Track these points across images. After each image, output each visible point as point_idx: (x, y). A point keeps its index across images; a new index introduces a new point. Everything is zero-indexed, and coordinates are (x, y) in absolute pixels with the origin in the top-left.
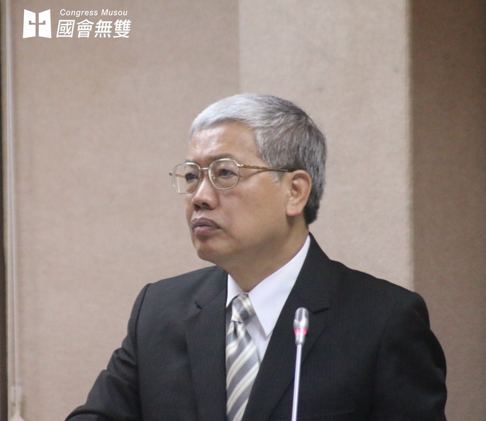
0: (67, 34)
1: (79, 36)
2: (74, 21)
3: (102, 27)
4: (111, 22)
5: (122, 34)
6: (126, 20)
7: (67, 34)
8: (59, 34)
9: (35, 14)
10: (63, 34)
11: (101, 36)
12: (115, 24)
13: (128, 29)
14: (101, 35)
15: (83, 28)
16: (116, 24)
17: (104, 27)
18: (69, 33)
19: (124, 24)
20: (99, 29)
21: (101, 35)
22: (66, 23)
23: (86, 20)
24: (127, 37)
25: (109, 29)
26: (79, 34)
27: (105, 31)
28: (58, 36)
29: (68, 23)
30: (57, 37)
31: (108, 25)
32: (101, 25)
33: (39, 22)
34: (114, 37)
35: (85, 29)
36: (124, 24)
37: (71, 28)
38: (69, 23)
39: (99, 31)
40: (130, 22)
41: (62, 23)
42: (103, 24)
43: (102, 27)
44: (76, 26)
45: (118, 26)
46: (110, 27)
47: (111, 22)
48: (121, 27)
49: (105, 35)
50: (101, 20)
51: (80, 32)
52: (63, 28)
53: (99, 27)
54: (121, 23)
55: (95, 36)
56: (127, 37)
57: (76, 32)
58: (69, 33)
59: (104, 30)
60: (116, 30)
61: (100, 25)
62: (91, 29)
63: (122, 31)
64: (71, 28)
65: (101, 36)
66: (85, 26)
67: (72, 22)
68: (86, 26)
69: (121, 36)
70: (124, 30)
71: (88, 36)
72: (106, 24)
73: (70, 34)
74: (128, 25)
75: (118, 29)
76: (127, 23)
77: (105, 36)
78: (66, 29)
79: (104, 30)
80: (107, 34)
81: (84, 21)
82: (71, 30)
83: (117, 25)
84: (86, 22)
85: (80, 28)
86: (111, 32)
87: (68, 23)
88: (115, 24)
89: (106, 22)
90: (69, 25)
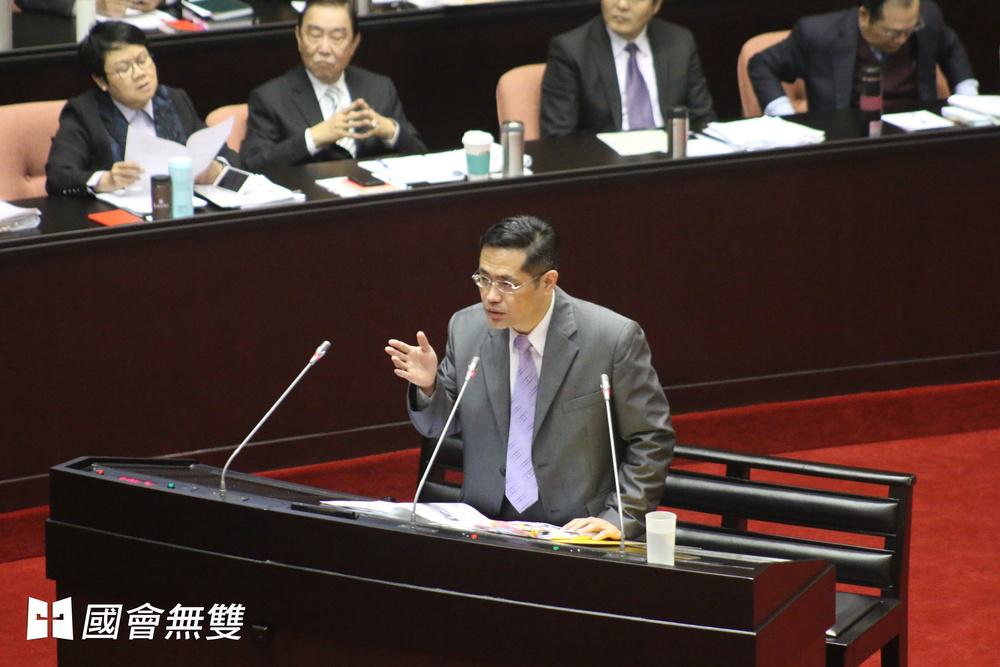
0: (105, 633)
1: (132, 637)
2: (120, 607)
3: (183, 618)
4: (202, 609)
7: (105, 633)
8: (88, 633)
9: (45, 604)
10: (96, 633)
11: (178, 637)
12: (209, 613)
13: (239, 621)
14: (178, 634)
15: (141, 620)
16: (212, 611)
17: (186, 618)
18: (110, 631)
20: (175, 623)
21: (178, 634)
22: (103, 610)
24: (237, 638)
25: (196, 623)
27: (188, 627)
28: (85, 636)
29: (107, 610)
30: (84, 638)
31: (194, 614)
32: (180, 615)
33: (54, 616)
34: (208, 638)
35: (144, 621)
36: (229, 611)
37: (115, 621)
38: (110, 611)
40: (244, 609)
41: (93, 610)
42: (183, 614)
43: (183, 618)
45: (217, 617)
46: (198, 618)
47: (202, 609)
48: (224, 619)
49: (187, 634)
50: (179, 605)
51: (133, 629)
52: (96, 621)
53: (175, 619)
54: (224, 611)
55: (167, 637)
56: (237, 638)
57: (125, 629)
58: (110, 631)
59: (185, 624)
60: (212, 623)
61: (176, 614)
62: (157, 623)
63: (226, 626)
64: (115, 621)
65: (178, 637)
67: (117, 610)
68: (148, 616)
69: (222, 636)
70: (229, 624)
71: (151, 637)
72: (190, 614)
73: (113, 633)
74: (237, 614)
75: (216, 622)
76: (236, 611)
77: (187, 636)
79: (185, 624)
80: (192, 632)
82: (114, 624)
84: (146, 609)
85: (134, 620)
86: (200, 628)
87: (107, 610)
88: (209, 613)
89: (191, 609)
90: (110, 614)
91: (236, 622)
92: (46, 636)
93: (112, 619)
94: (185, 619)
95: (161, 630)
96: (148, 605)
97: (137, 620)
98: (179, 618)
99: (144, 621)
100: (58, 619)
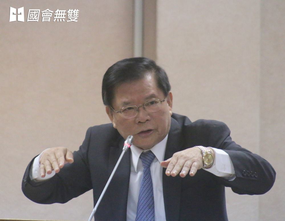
0: (35, 19)
2: (39, 10)
3: (59, 14)
4: (65, 11)
5: (73, 19)
6: (75, 10)
9: (15, 9)
12: (68, 12)
13: (77, 15)
16: (69, 12)
19: (74, 12)
21: (58, 19)
23: (48, 10)
24: (76, 21)
25: (64, 16)
26: (43, 19)
27: (61, 17)
28: (28, 20)
30: (28, 21)
33: (18, 14)
36: (74, 12)
39: (57, 17)
40: (79, 11)
43: (59, 14)
44: (41, 13)
45: (70, 14)
46: (64, 14)
47: (65, 11)
48: (72, 14)
50: (58, 10)
51: (43, 18)
53: (57, 14)
54: (72, 12)
55: (54, 21)
56: (76, 21)
57: (41, 18)
58: (36, 19)
59: (60, 16)
60: (69, 16)
61: (57, 13)
62: (51, 16)
65: (58, 21)
66: (47, 14)
69: (72, 20)
71: (49, 21)
73: (37, 19)
74: (76, 14)
78: (34, 16)
79: (60, 16)
81: (47, 10)
83: (69, 13)
85: (44, 15)
89: (62, 11)
90: (36, 13)
91: (76, 15)
92: (15, 20)
93: (37, 14)
94: (60, 14)
95: (52, 18)
96: (48, 10)
97: (45, 15)
98: (58, 14)
99: (47, 15)
100: (19, 14)
